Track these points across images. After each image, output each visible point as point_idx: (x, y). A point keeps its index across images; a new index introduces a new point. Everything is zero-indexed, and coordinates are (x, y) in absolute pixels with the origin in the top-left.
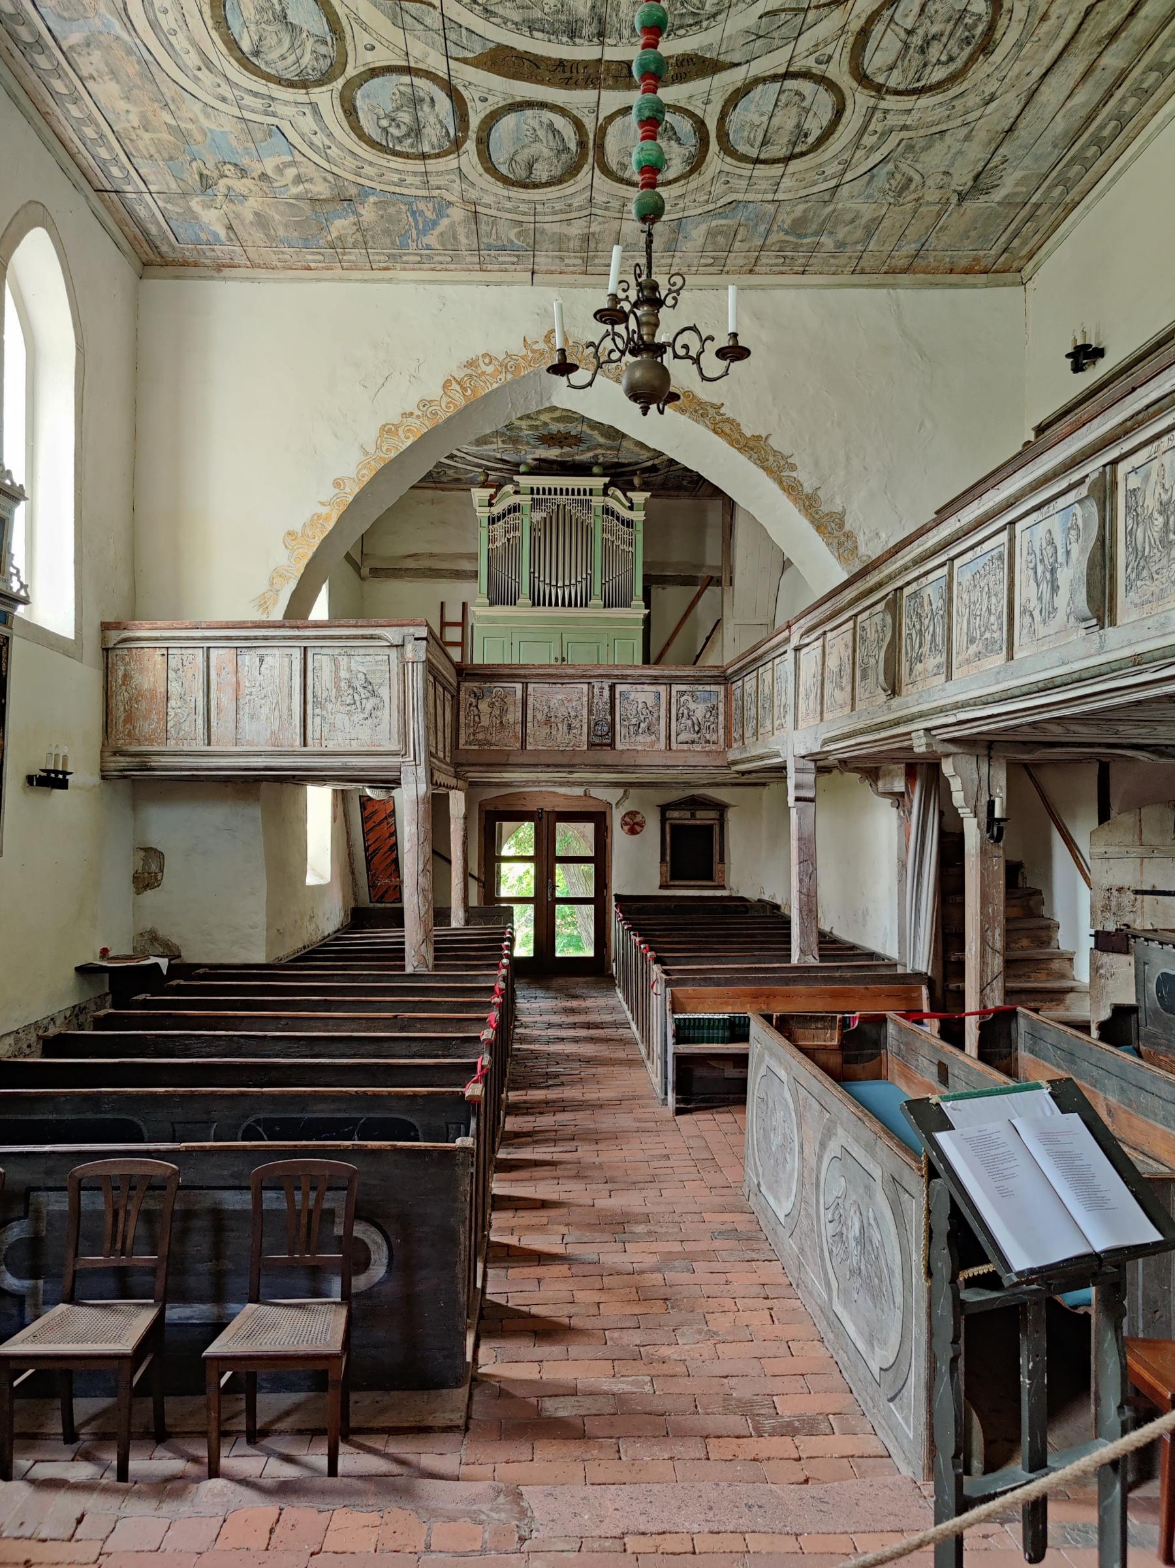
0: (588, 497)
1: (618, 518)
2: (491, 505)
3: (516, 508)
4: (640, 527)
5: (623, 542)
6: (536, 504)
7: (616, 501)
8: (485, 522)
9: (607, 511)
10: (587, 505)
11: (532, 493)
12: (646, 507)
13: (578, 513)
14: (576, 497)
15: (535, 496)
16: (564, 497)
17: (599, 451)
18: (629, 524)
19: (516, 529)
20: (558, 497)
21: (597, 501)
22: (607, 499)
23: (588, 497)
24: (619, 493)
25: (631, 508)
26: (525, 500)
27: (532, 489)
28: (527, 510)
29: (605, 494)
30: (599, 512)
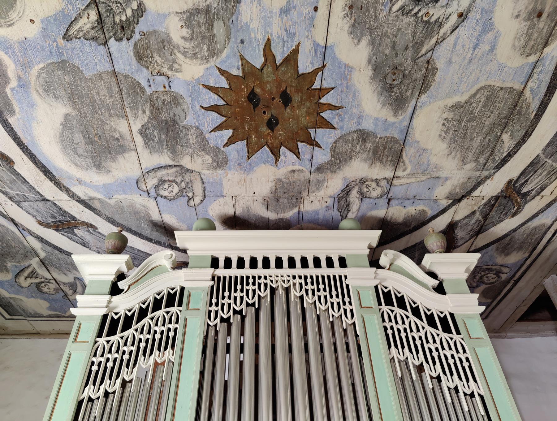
0: (337, 271)
1: (416, 312)
2: (115, 290)
3: (174, 298)
4: (478, 329)
5: (448, 370)
6: (219, 287)
7: (402, 275)
8: (89, 330)
9: (386, 297)
10: (339, 286)
11: (215, 263)
12: (475, 281)
13: (320, 305)
14: (311, 271)
15: (221, 272)
16: (286, 271)
17: (358, 168)
18: (447, 323)
19: (169, 342)
20: (273, 271)
21: (361, 278)
22: (380, 271)
23: (337, 271)
24: (405, 262)
25: (440, 289)
26: (197, 280)
27: (215, 263)
28: (199, 300)
29: (374, 263)
30: (370, 299)
